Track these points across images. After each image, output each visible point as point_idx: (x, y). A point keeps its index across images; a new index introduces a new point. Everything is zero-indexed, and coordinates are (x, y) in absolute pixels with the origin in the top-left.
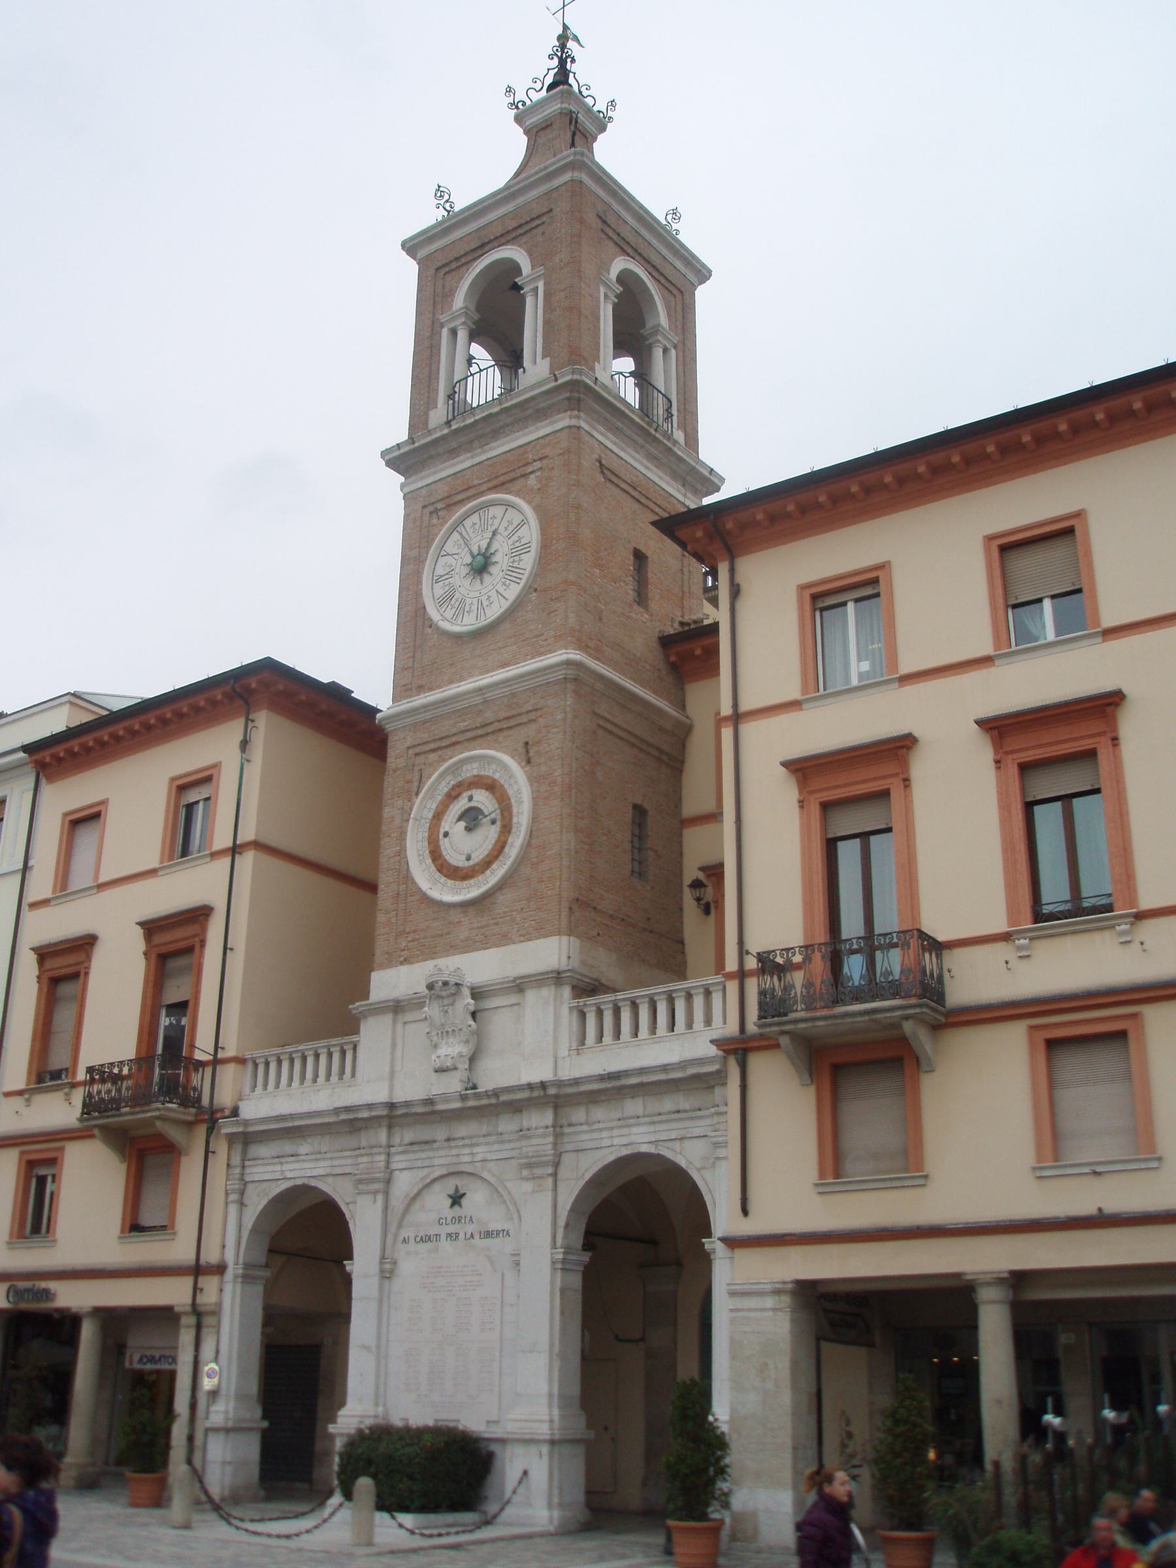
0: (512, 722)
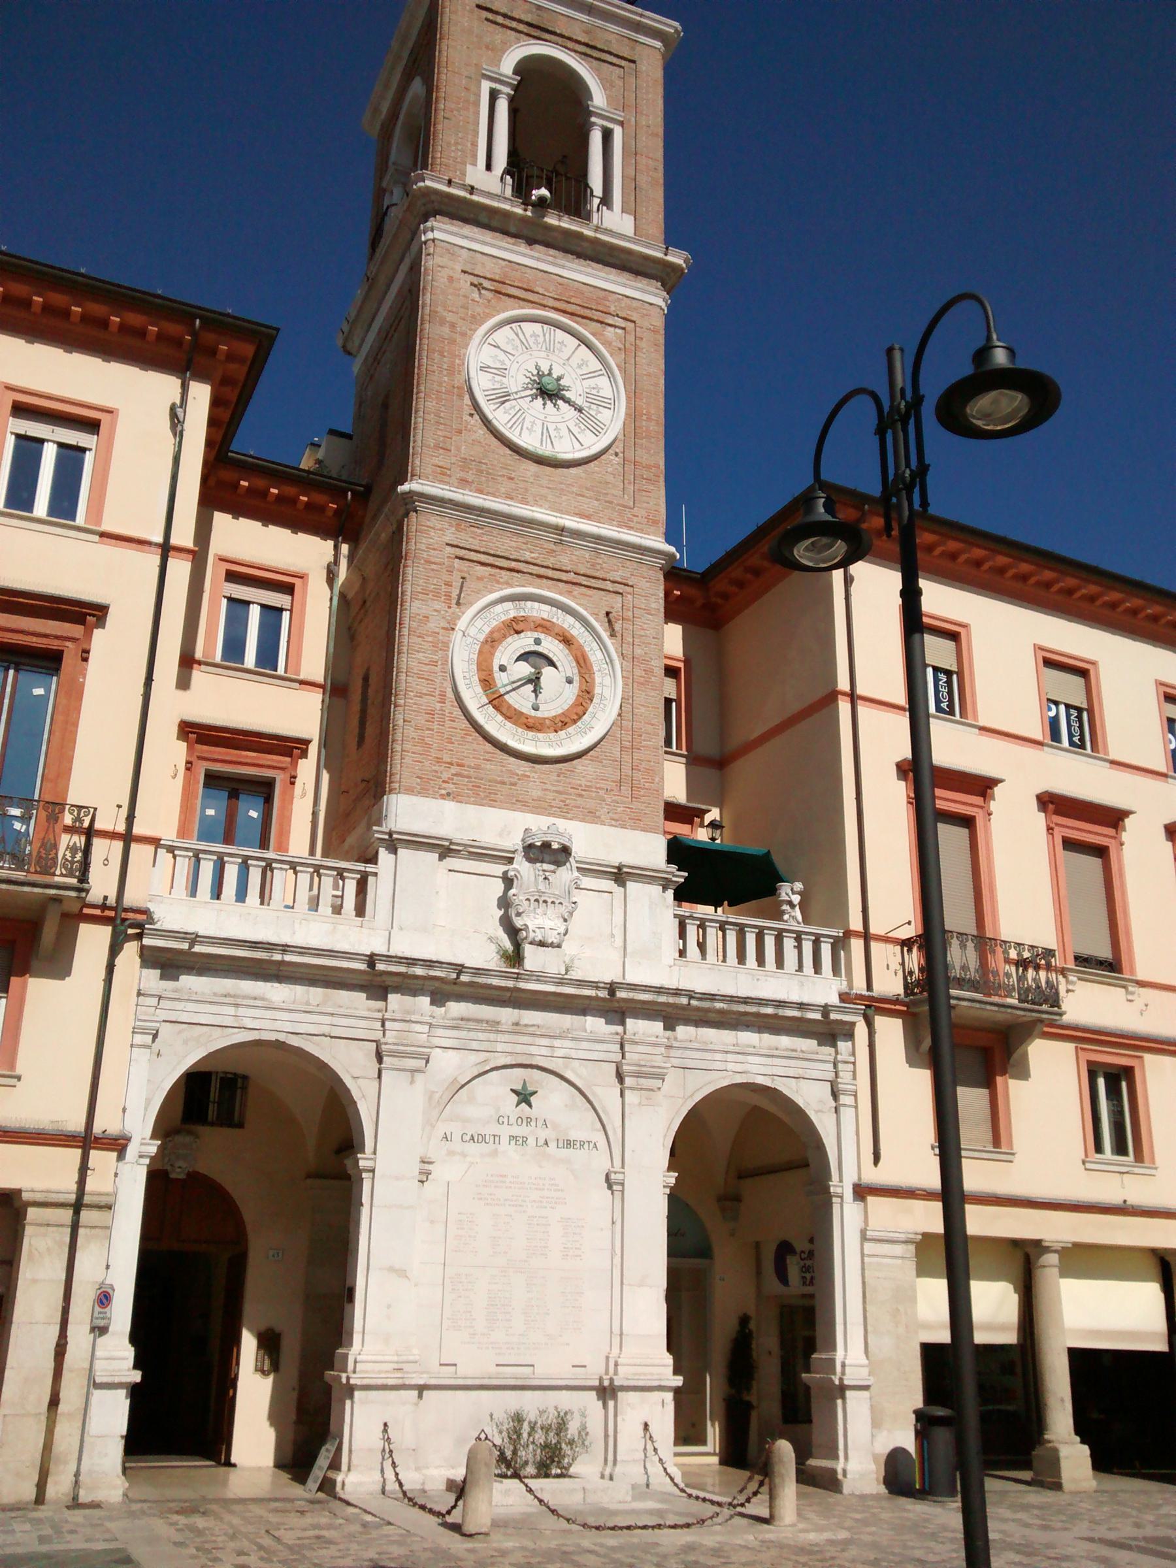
0: (593, 583)
